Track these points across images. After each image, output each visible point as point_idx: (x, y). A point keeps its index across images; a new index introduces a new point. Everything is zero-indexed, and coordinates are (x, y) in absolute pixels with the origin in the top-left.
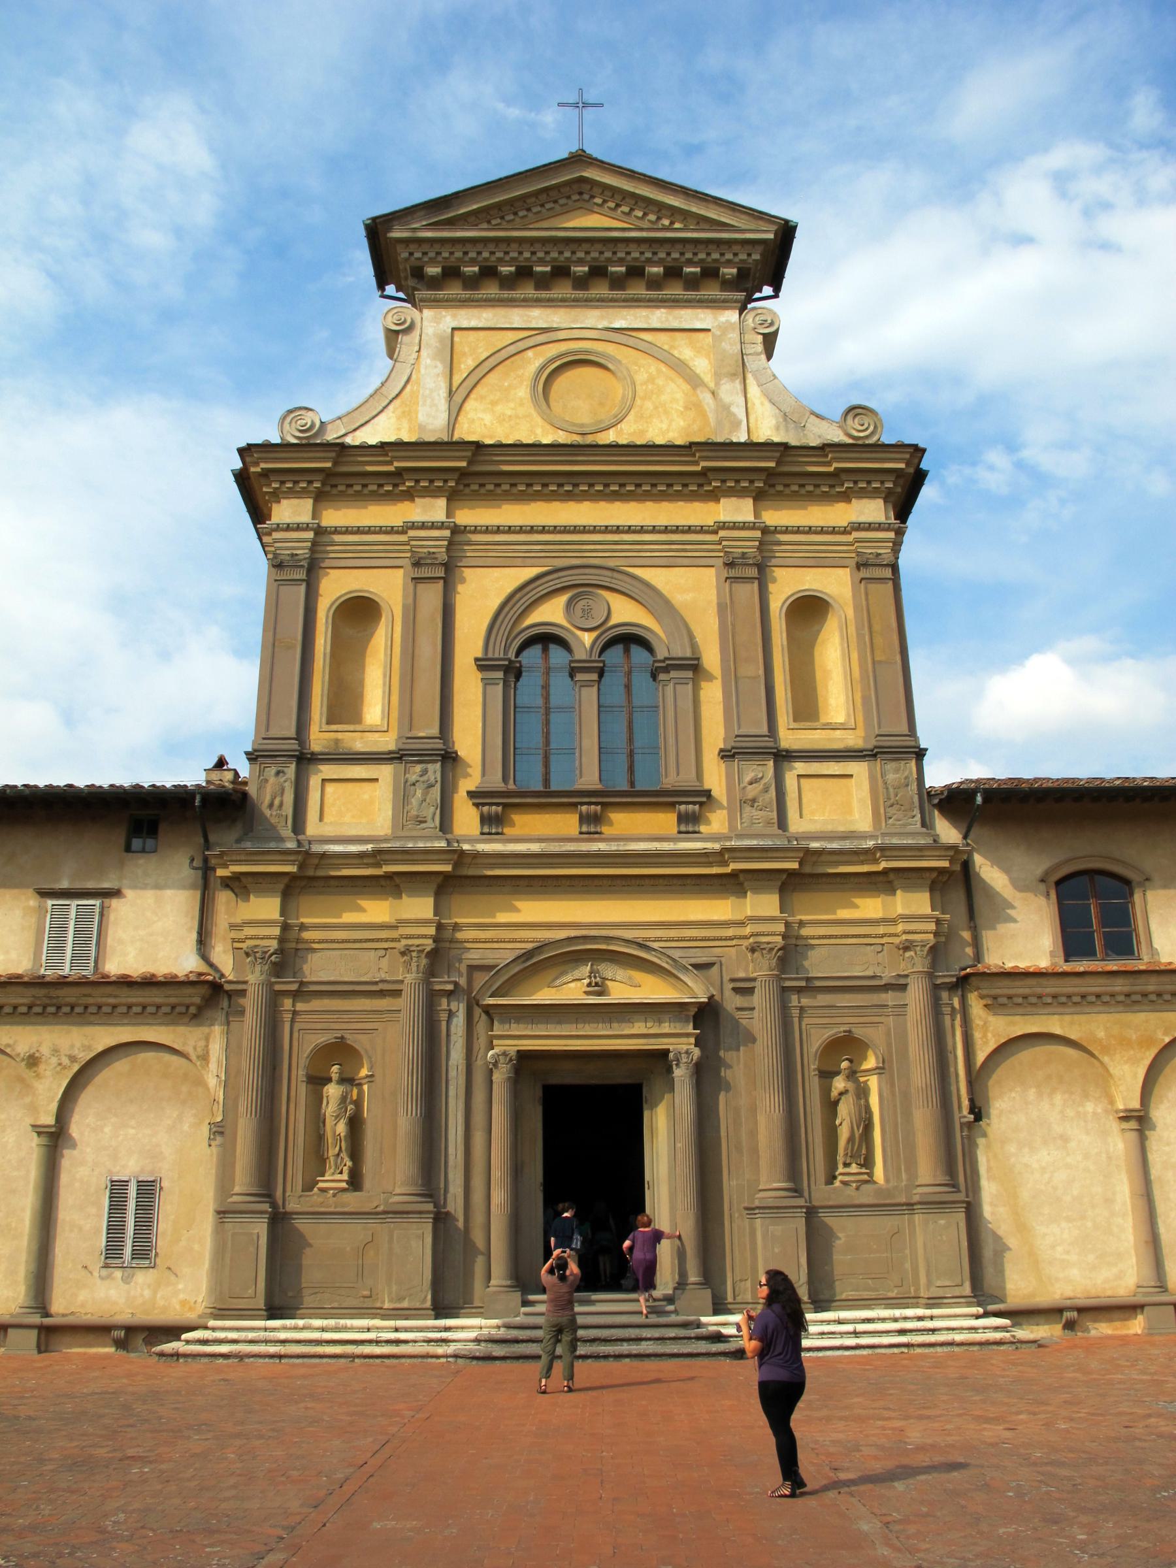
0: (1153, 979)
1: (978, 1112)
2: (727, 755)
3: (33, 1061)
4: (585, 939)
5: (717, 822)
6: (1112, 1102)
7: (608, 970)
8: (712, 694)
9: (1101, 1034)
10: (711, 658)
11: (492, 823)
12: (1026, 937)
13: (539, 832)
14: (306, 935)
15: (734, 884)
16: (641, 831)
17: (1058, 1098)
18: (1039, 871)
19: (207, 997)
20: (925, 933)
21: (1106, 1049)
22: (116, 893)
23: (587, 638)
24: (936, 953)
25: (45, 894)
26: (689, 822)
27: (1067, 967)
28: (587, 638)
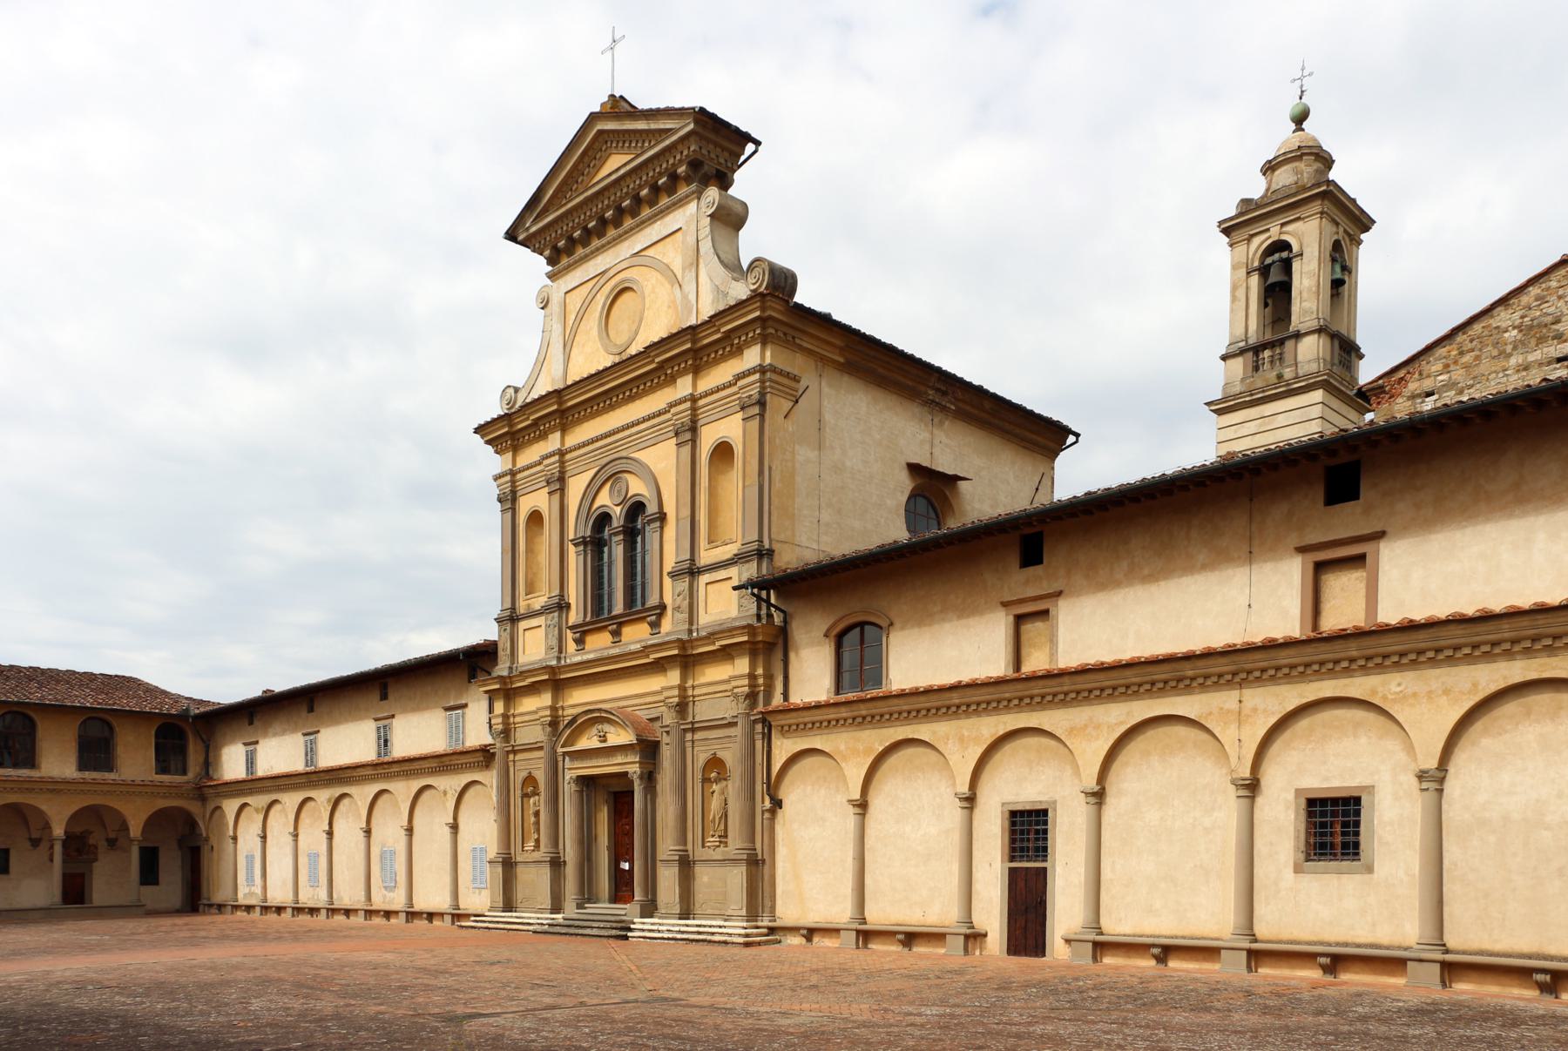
0: (862, 706)
1: (777, 804)
2: (673, 575)
3: (445, 793)
4: (599, 710)
5: (667, 625)
6: (954, 784)
7: (606, 727)
8: (670, 531)
9: (842, 747)
10: (670, 509)
11: (580, 641)
12: (812, 674)
13: (599, 643)
14: (518, 719)
15: (659, 666)
16: (636, 635)
17: (823, 792)
18: (824, 628)
19: (484, 756)
20: (743, 687)
21: (845, 758)
22: (465, 706)
23: (618, 509)
24: (752, 697)
25: (447, 709)
26: (655, 625)
27: (842, 698)
28: (618, 509)
